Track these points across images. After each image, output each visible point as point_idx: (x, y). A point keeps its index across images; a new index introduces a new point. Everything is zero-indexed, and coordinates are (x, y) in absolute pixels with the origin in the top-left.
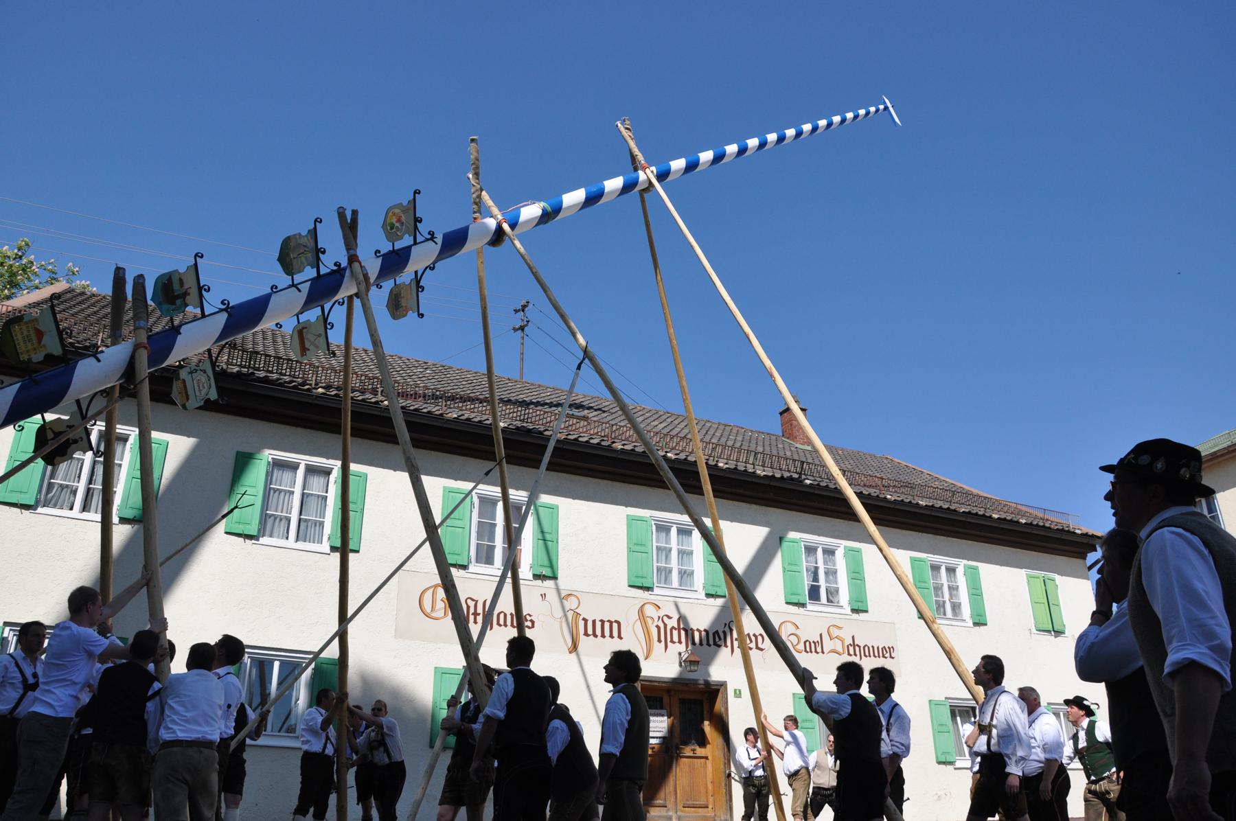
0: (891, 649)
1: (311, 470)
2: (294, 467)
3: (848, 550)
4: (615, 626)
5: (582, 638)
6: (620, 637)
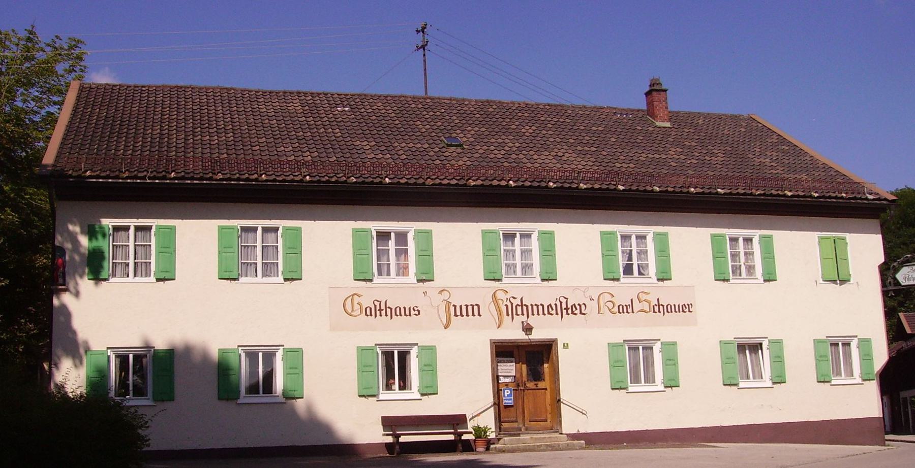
0: (689, 306)
1: (266, 230)
2: (127, 229)
3: (656, 235)
4: (476, 308)
5: (453, 318)
6: (479, 315)
